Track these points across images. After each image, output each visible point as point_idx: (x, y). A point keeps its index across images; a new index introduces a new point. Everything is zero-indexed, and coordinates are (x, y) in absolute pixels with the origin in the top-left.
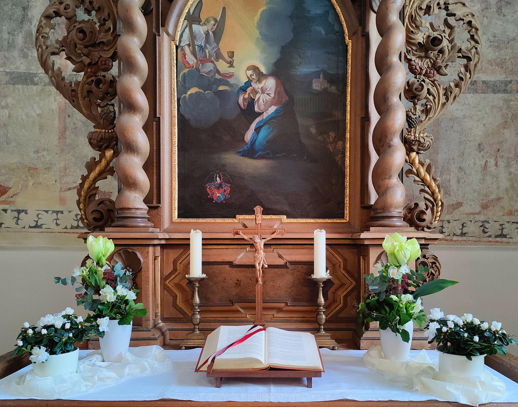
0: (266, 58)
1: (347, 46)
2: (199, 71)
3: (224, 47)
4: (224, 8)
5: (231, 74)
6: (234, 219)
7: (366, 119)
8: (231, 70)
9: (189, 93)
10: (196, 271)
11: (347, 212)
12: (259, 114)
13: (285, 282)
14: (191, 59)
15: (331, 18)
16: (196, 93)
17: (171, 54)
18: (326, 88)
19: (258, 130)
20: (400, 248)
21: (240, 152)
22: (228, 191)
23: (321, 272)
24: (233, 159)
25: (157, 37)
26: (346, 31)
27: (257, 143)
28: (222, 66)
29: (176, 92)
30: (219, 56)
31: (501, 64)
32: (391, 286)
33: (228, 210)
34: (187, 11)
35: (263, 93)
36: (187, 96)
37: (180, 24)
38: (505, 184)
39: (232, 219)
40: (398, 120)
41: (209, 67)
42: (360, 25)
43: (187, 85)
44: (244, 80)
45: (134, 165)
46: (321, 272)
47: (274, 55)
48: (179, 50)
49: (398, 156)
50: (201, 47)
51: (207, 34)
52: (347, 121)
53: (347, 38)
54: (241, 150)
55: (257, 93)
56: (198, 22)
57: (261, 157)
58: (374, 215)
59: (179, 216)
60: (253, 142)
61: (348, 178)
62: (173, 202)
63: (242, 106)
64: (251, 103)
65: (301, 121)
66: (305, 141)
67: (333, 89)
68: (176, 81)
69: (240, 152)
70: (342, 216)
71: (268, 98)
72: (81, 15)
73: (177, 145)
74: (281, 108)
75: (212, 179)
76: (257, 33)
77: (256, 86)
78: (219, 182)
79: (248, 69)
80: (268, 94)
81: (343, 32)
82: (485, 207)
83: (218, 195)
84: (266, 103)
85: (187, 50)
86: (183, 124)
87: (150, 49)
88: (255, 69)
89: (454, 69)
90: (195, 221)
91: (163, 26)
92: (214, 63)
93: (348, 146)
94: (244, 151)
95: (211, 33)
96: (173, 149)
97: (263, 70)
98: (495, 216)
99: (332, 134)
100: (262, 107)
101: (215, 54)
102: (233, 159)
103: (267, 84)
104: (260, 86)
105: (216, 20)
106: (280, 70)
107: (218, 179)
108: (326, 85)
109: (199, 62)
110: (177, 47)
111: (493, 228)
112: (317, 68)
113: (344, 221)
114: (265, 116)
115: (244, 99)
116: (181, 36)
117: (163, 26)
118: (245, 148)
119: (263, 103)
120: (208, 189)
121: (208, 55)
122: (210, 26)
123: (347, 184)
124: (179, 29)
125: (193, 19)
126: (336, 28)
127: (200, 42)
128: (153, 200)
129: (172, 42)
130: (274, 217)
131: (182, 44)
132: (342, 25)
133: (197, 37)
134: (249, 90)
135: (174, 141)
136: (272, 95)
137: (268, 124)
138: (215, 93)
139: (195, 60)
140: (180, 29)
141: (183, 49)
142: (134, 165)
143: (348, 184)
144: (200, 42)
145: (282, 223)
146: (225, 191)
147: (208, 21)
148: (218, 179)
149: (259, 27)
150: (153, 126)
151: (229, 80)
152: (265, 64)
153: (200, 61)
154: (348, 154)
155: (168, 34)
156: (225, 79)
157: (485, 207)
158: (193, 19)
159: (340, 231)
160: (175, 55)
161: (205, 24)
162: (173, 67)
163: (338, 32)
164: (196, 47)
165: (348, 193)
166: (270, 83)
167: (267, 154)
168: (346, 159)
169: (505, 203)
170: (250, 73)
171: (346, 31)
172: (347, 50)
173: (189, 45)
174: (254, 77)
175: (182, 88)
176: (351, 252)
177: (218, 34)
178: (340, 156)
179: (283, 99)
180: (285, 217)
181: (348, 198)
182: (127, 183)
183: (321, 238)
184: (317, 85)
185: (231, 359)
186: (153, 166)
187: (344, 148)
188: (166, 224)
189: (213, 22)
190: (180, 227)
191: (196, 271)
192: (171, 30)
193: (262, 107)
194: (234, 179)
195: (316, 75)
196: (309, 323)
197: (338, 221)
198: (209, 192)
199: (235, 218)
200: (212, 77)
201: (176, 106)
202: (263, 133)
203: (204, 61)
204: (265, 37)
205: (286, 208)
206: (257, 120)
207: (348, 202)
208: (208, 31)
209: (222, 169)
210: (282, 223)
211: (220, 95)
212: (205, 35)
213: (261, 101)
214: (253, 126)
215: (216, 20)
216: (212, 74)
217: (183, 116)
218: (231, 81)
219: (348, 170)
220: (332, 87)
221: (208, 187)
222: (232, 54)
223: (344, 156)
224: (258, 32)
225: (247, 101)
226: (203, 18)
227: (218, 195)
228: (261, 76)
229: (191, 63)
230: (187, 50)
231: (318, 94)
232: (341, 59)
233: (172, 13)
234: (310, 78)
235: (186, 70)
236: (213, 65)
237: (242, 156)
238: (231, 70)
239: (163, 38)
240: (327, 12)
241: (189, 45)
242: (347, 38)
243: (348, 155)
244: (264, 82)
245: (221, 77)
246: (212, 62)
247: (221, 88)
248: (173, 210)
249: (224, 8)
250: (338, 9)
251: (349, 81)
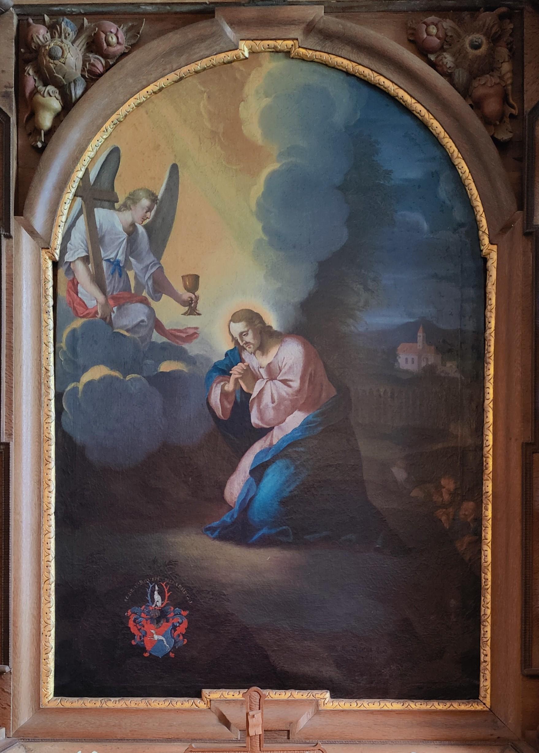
0: (280, 290)
1: (485, 260)
2: (111, 324)
3: (176, 262)
4: (174, 169)
5: (191, 332)
6: (197, 701)
8: (192, 321)
9: (86, 378)
11: (485, 683)
12: (262, 432)
14: (90, 295)
15: (444, 190)
16: (103, 379)
17: (39, 281)
18: (430, 370)
19: (258, 472)
21: (212, 530)
22: (182, 629)
24: (196, 548)
25: (4, 242)
26: (484, 223)
27: (256, 504)
28: (169, 312)
29: (52, 379)
30: (161, 286)
33: (181, 677)
34: (80, 174)
35: (272, 377)
36: (81, 387)
37: (64, 208)
39: (191, 700)
41: (136, 313)
42: (520, 207)
43: (81, 361)
44: (226, 346)
47: (300, 283)
48: (61, 271)
50: (115, 264)
51: (131, 231)
52: (486, 449)
53: (486, 240)
54: (215, 524)
55: (256, 378)
56: (110, 201)
57: (266, 542)
59: (59, 692)
60: (246, 504)
61: (489, 597)
62: (43, 656)
63: (219, 412)
64: (242, 404)
65: (367, 448)
66: (379, 502)
67: (451, 368)
68: (52, 349)
69: (212, 530)
70: (473, 693)
71: (284, 390)
73: (53, 510)
74: (316, 416)
75: (142, 599)
76: (256, 229)
77: (255, 361)
78: (159, 604)
79: (236, 318)
80: (284, 382)
81: (475, 225)
83: (156, 637)
84: (279, 404)
85: (82, 273)
86: (70, 455)
88: (252, 318)
90: (98, 705)
91: (19, 212)
92: (148, 304)
93: (489, 513)
94: (225, 526)
95: (141, 229)
96: (44, 520)
97: (273, 320)
99: (448, 484)
100: (270, 414)
101: (150, 283)
102: (196, 548)
103: (280, 357)
104: (265, 361)
105: (153, 198)
106: (314, 321)
107: (157, 597)
108: (432, 359)
109: (111, 302)
110: (56, 265)
112: (410, 315)
113: (480, 707)
114: (277, 436)
115: (224, 395)
116: (67, 237)
117: (19, 212)
118: (227, 518)
119: (271, 405)
120: (131, 624)
121: (133, 283)
122: (139, 213)
123: (487, 611)
124: (62, 219)
125: (97, 194)
126: (458, 215)
127: (114, 251)
129: (43, 252)
130: (297, 695)
131: (68, 258)
132: (472, 209)
133: (107, 239)
134: (236, 371)
135: (45, 500)
136: (296, 384)
137: (286, 456)
138: (148, 378)
139: (101, 298)
140: (64, 219)
141: (70, 271)
143: (489, 612)
144: (114, 251)
145: (318, 712)
146: (174, 628)
147: (133, 199)
148: (157, 597)
149: (262, 212)
151: (186, 346)
152: (277, 306)
153: (113, 298)
154: (488, 534)
155: (32, 232)
156: (175, 344)
158: (97, 194)
159: (468, 733)
160: (51, 283)
161: (125, 207)
162: (44, 316)
163: (461, 225)
164: (104, 264)
165: (489, 635)
166: (290, 355)
167: (284, 533)
168: (485, 547)
170: (238, 327)
171: (484, 223)
172: (485, 271)
173: (85, 260)
174: (249, 338)
175: (68, 367)
177: (159, 231)
178: (467, 539)
179: (324, 395)
180: (327, 695)
181: (488, 649)
184: (408, 360)
187: (479, 520)
188: (24, 715)
189: (145, 202)
190: (61, 723)
192: (39, 220)
193: (270, 414)
194: (199, 601)
195: (408, 333)
197: (463, 707)
198: (134, 630)
199: (199, 695)
200: (143, 339)
201: (53, 414)
202: (272, 481)
203: (123, 298)
204: (277, 239)
205: (329, 671)
206: (258, 447)
207: (488, 659)
208: (133, 225)
209: (167, 572)
210: (318, 712)
211: (166, 384)
212: (125, 236)
213: (267, 399)
214: (247, 462)
215: (153, 198)
216: (143, 332)
217: (70, 438)
218: (193, 348)
219: (489, 576)
220: (448, 364)
221: (133, 618)
222: (193, 282)
223: (478, 540)
224: (259, 226)
225: (232, 398)
226: (122, 191)
227: (156, 637)
228: (266, 337)
229: (91, 304)
230: (82, 273)
231: (413, 380)
232: (471, 292)
233: (41, 181)
234: (387, 344)
235: (78, 323)
236: (146, 310)
237: (222, 538)
238: (192, 321)
239: (18, 243)
240: (435, 175)
241: (85, 260)
242: (486, 240)
243: (489, 536)
244: (273, 351)
245: (165, 339)
246: (144, 301)
247: (166, 367)
248: (43, 677)
249: (174, 169)
250: (463, 168)
251: (492, 349)
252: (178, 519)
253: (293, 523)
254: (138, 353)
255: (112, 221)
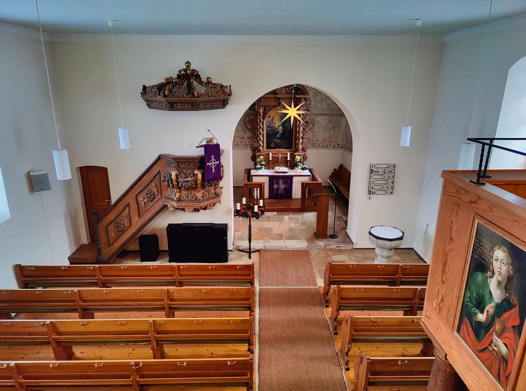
7: (296, 134)
10: (271, 159)
13: (283, 159)
20: (298, 158)
23: (289, 159)
24: (275, 140)
28: (273, 125)
31: (329, 110)
32: (297, 162)
38: (328, 136)
40: (301, 135)
45: (261, 142)
46: (289, 159)
49: (301, 141)
58: (297, 150)
72: (251, 117)
82: (324, 140)
87: (263, 124)
89: (311, 126)
98: (326, 143)
111: (325, 145)
125: (269, 117)
128: (263, 147)
142: (261, 142)
150: (263, 136)
157: (324, 140)
166: (281, 127)
169: (328, 140)
176: (293, 157)
182: (260, 145)
183: (289, 154)
185: (278, 171)
186: (263, 142)
191: (271, 159)
196: (286, 166)
209: (273, 142)
252: (275, 138)
253: (281, 138)
254: (271, 127)
255: (270, 119)
